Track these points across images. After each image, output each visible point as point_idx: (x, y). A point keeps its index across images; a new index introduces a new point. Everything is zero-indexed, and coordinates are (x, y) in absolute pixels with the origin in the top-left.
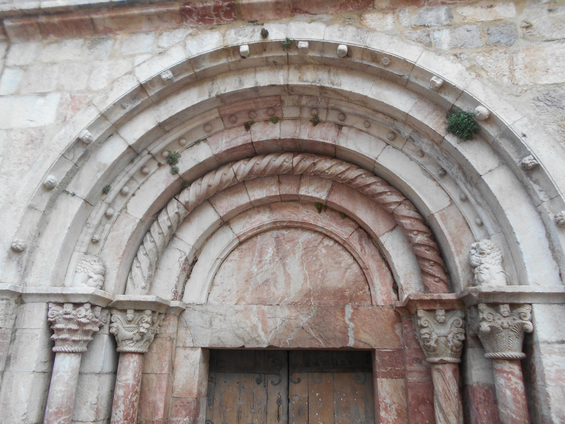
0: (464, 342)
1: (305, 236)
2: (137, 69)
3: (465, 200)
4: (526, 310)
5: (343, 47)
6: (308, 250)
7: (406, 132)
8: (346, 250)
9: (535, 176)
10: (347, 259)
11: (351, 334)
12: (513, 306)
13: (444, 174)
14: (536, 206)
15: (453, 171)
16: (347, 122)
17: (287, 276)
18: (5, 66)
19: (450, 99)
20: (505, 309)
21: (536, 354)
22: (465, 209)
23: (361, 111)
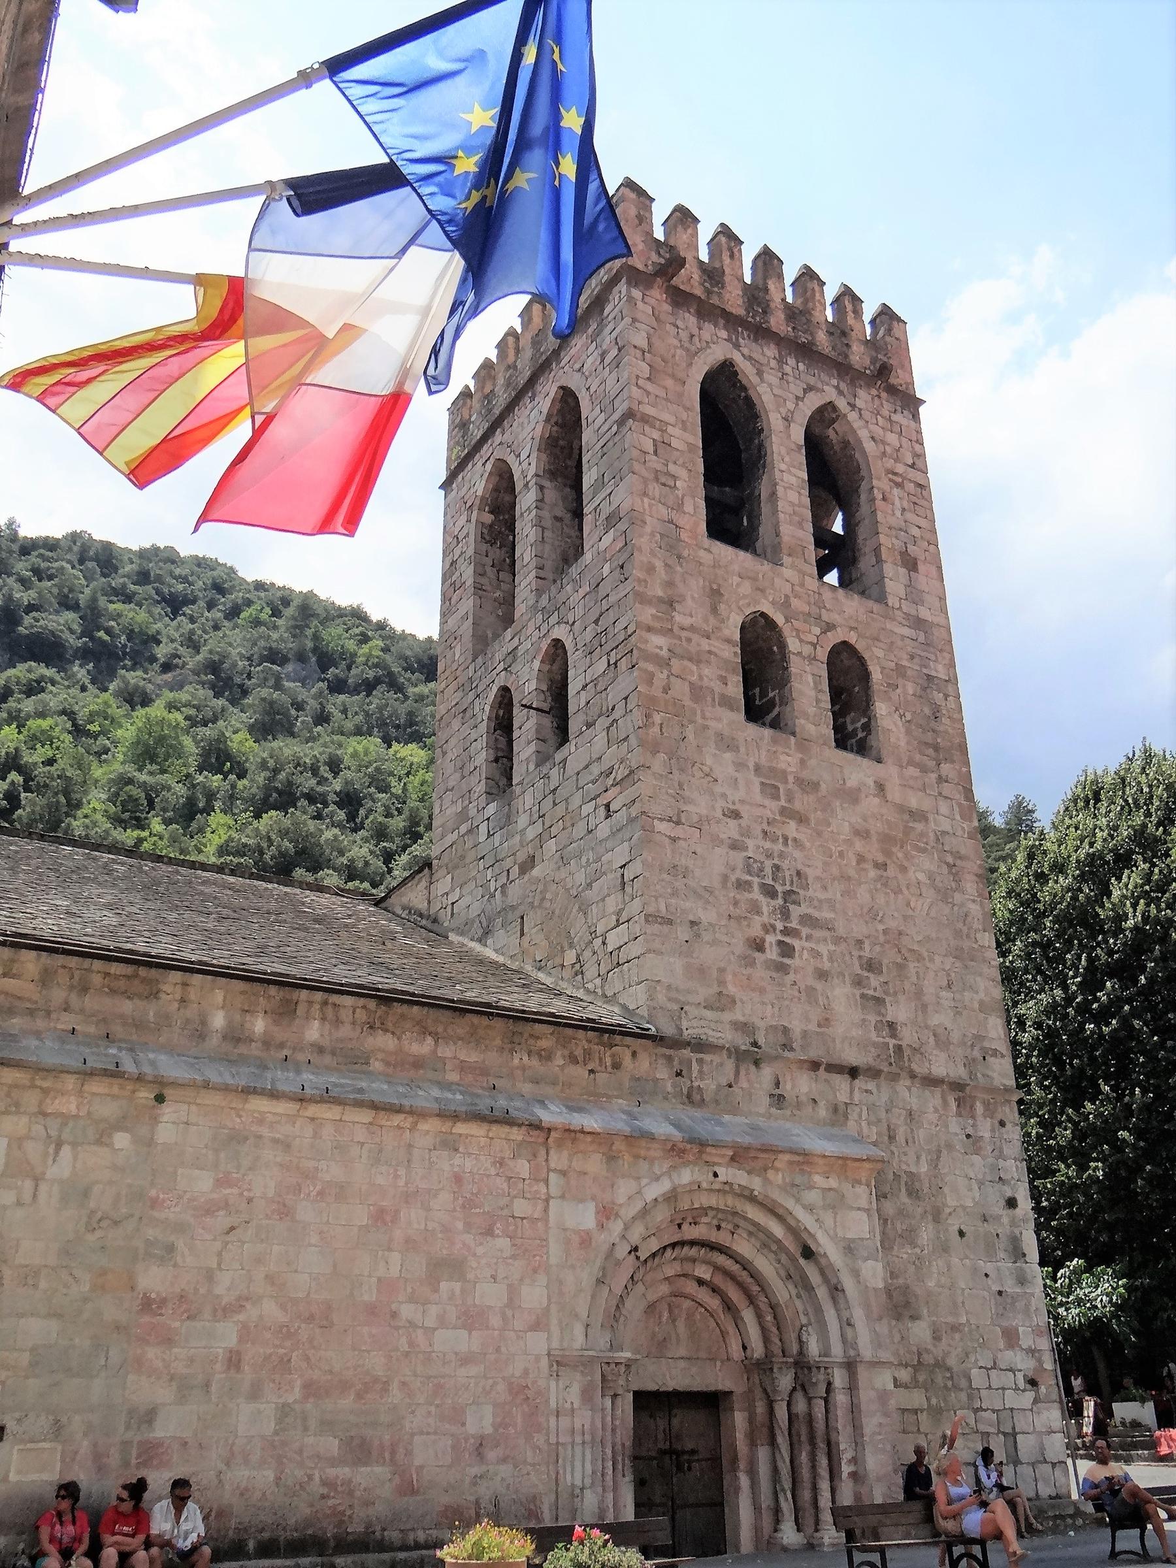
0: (794, 1389)
1: (687, 1304)
2: (643, 1191)
3: (799, 1296)
4: (829, 1371)
5: (756, 1193)
6: (690, 1317)
7: (774, 1247)
8: (712, 1316)
9: (840, 1294)
10: (713, 1324)
11: (720, 1379)
12: (826, 1368)
13: (789, 1277)
14: (837, 1310)
15: (797, 1278)
16: (739, 1231)
17: (678, 1335)
18: (549, 1170)
19: (805, 1236)
20: (822, 1370)
21: (832, 1394)
22: (798, 1303)
23: (751, 1228)
